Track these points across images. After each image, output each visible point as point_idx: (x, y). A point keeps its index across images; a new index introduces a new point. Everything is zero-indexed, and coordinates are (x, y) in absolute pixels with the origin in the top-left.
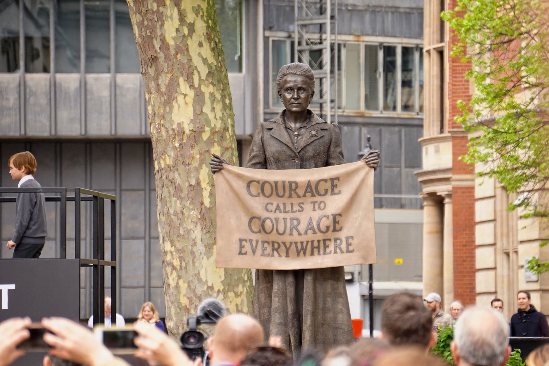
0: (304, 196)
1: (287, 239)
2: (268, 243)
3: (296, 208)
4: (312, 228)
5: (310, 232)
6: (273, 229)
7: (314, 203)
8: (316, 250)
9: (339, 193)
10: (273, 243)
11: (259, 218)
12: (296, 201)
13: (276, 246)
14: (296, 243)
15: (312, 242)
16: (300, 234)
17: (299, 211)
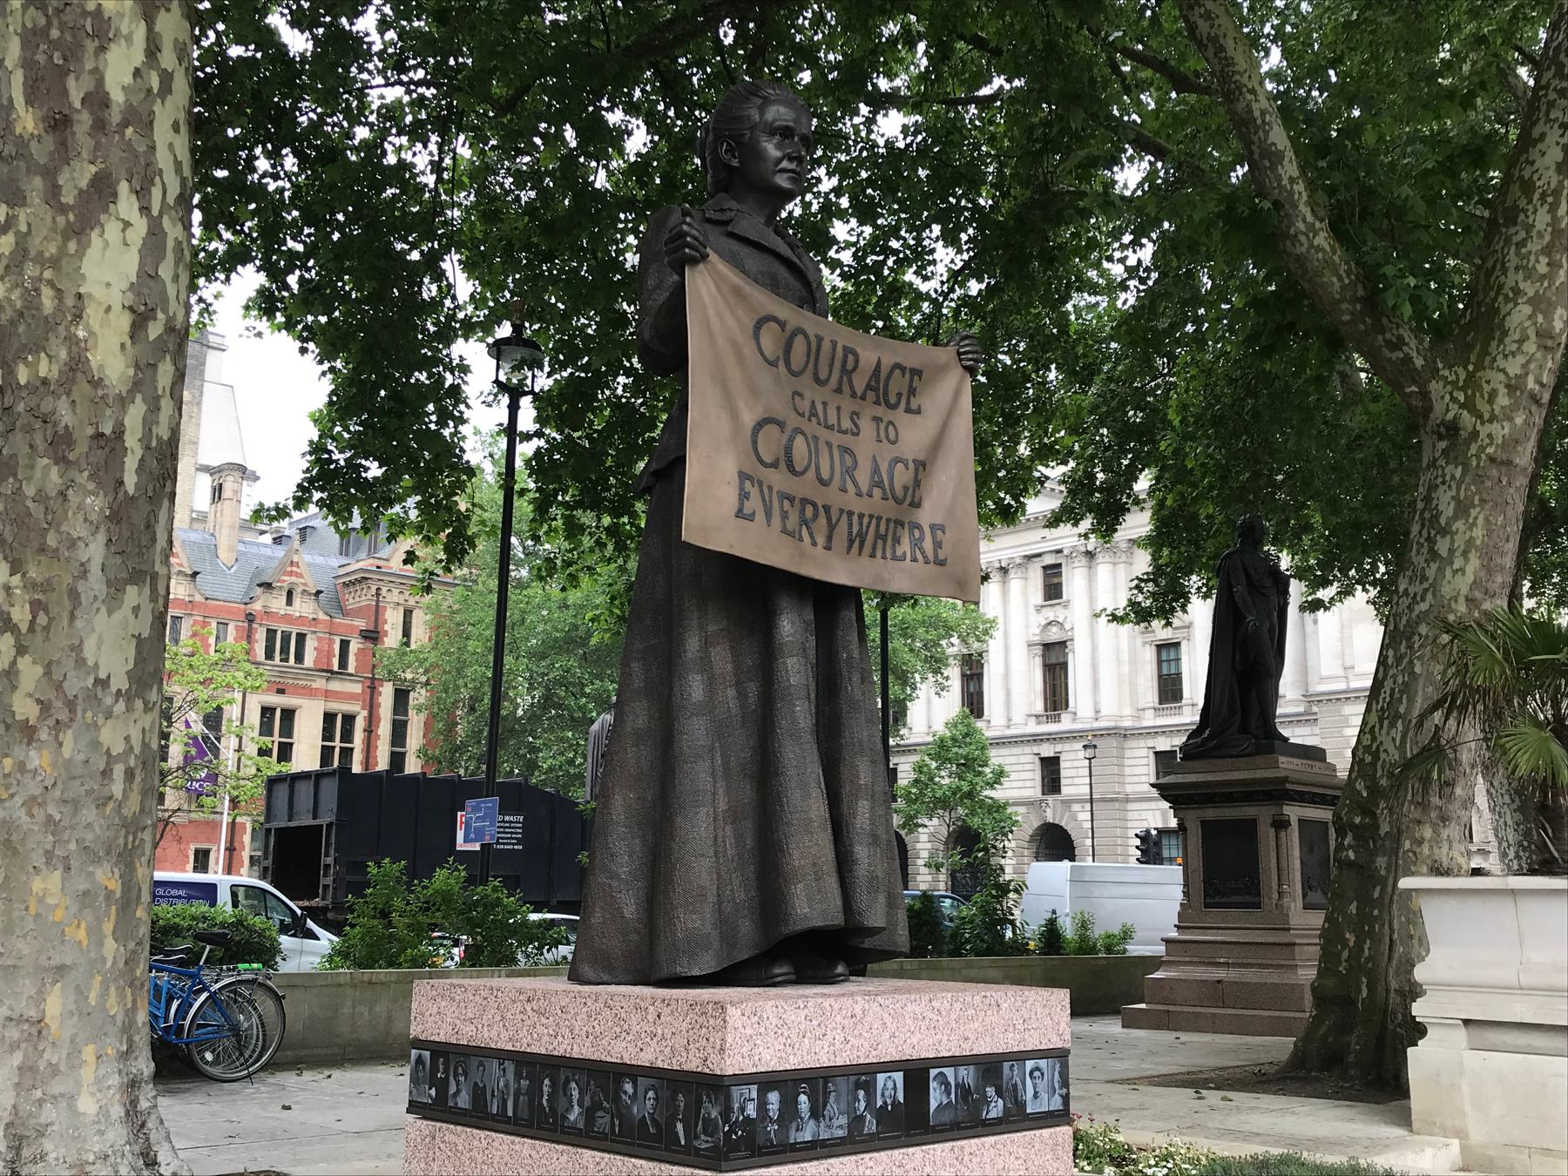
0: (863, 398)
1: (832, 496)
2: (791, 499)
3: (846, 424)
4: (879, 484)
5: (877, 492)
6: (809, 465)
7: (877, 420)
8: (880, 542)
9: (918, 412)
10: (804, 501)
11: (781, 425)
12: (848, 405)
13: (809, 510)
14: (850, 514)
15: (879, 519)
16: (859, 494)
17: (853, 434)
